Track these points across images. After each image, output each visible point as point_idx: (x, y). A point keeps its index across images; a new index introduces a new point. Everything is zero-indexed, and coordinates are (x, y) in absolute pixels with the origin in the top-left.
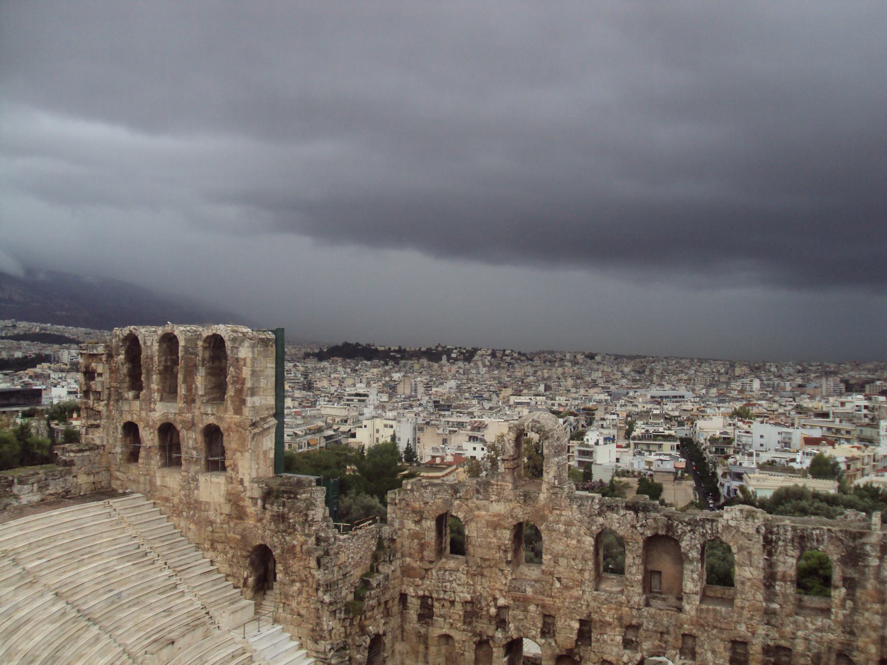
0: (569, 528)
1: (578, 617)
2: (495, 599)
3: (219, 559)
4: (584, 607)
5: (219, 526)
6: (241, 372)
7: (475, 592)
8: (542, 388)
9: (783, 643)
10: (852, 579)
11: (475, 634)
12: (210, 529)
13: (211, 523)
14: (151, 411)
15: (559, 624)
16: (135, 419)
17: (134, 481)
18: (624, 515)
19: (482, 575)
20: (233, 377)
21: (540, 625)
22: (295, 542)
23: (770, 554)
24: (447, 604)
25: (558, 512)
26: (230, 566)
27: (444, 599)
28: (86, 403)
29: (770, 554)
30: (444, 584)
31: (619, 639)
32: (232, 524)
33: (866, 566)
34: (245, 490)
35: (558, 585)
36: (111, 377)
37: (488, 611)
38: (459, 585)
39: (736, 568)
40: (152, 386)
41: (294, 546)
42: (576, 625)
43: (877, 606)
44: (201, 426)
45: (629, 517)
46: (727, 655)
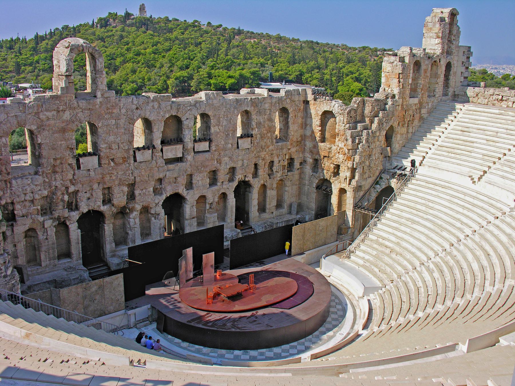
0: (119, 121)
1: (127, 183)
2: (67, 188)
4: (131, 175)
7: (50, 187)
9: (233, 165)
10: (260, 123)
11: (54, 219)
15: (116, 190)
18: (153, 106)
19: (55, 172)
21: (102, 197)
23: (227, 117)
24: (27, 204)
25: (110, 111)
27: (26, 200)
29: (227, 117)
30: (25, 188)
31: (152, 190)
33: (266, 115)
35: (112, 164)
37: (63, 200)
38: (36, 185)
39: (212, 128)
42: (126, 189)
43: (269, 135)
45: (156, 107)
46: (208, 180)
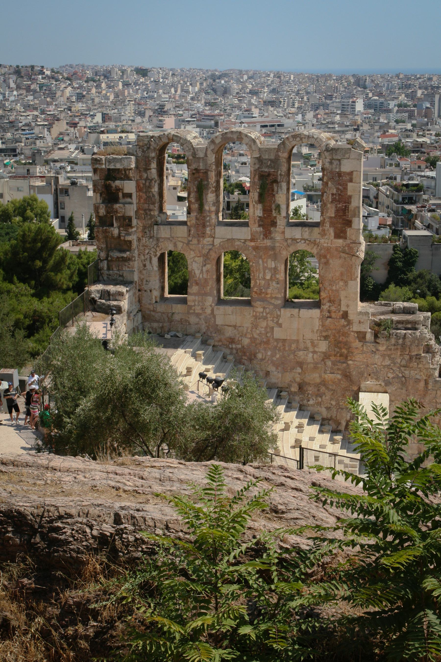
3: (311, 402)
5: (312, 366)
6: (346, 189)
8: (98, 118)
12: (299, 370)
13: (301, 364)
14: (203, 237)
16: (180, 248)
17: (181, 321)
20: (333, 194)
22: (418, 377)
26: (328, 409)
28: (105, 232)
32: (329, 363)
34: (349, 323)
36: (139, 198)
40: (207, 208)
41: (417, 381)
44: (285, 254)
